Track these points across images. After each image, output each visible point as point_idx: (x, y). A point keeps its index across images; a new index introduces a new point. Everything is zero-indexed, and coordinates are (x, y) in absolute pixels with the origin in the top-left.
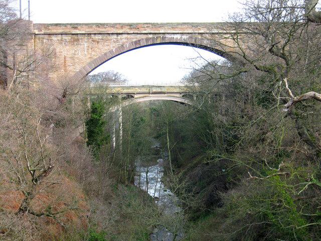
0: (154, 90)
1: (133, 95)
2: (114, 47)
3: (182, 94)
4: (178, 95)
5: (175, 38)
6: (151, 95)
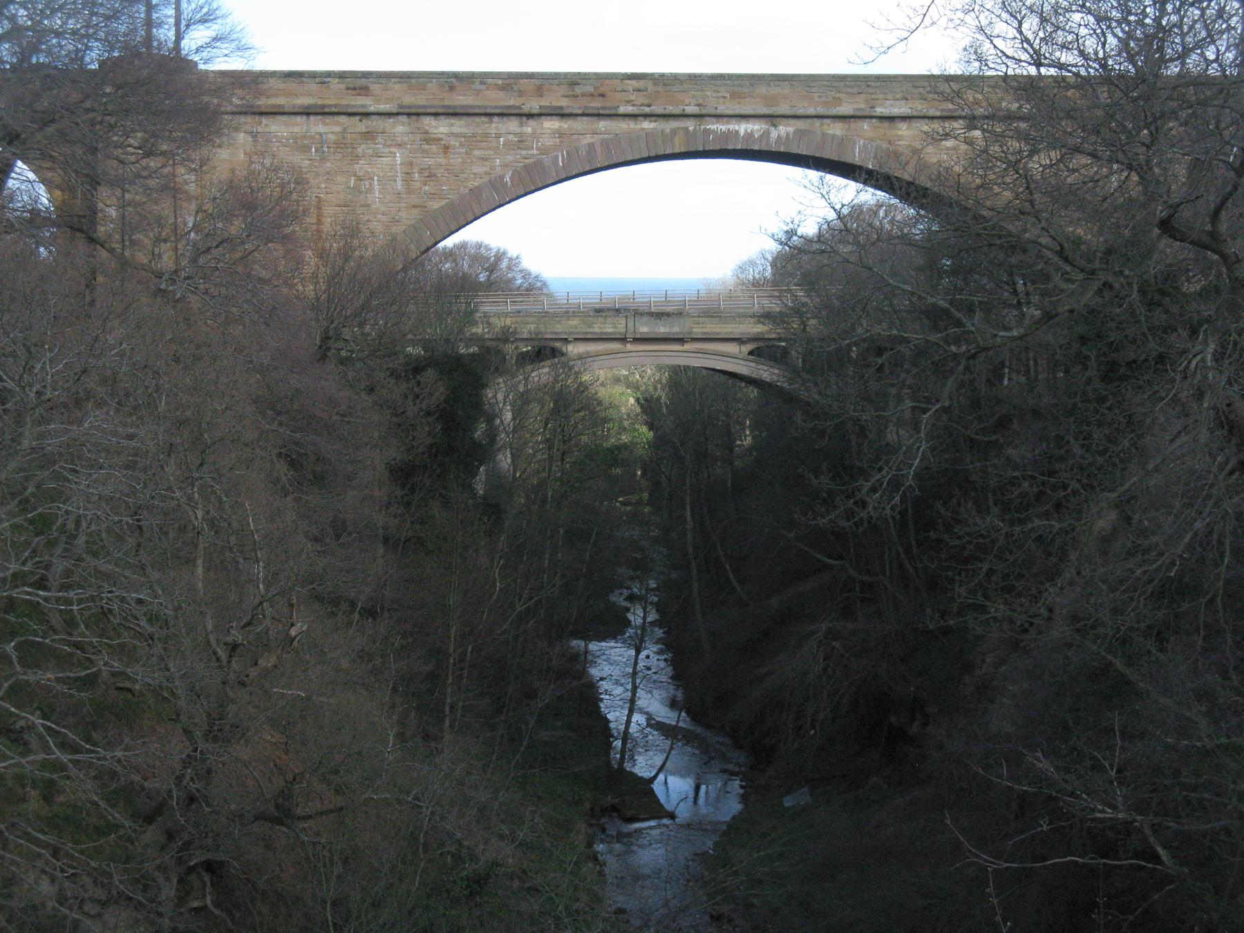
0: (644, 329)
1: (557, 345)
2: (505, 166)
3: (749, 347)
4: (732, 348)
5: (742, 133)
6: (629, 347)
